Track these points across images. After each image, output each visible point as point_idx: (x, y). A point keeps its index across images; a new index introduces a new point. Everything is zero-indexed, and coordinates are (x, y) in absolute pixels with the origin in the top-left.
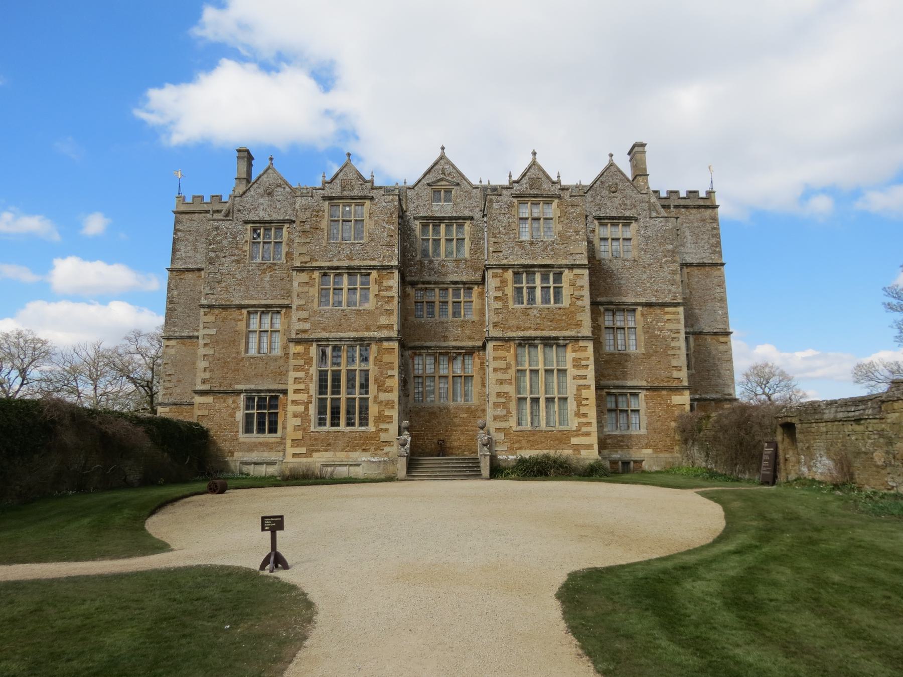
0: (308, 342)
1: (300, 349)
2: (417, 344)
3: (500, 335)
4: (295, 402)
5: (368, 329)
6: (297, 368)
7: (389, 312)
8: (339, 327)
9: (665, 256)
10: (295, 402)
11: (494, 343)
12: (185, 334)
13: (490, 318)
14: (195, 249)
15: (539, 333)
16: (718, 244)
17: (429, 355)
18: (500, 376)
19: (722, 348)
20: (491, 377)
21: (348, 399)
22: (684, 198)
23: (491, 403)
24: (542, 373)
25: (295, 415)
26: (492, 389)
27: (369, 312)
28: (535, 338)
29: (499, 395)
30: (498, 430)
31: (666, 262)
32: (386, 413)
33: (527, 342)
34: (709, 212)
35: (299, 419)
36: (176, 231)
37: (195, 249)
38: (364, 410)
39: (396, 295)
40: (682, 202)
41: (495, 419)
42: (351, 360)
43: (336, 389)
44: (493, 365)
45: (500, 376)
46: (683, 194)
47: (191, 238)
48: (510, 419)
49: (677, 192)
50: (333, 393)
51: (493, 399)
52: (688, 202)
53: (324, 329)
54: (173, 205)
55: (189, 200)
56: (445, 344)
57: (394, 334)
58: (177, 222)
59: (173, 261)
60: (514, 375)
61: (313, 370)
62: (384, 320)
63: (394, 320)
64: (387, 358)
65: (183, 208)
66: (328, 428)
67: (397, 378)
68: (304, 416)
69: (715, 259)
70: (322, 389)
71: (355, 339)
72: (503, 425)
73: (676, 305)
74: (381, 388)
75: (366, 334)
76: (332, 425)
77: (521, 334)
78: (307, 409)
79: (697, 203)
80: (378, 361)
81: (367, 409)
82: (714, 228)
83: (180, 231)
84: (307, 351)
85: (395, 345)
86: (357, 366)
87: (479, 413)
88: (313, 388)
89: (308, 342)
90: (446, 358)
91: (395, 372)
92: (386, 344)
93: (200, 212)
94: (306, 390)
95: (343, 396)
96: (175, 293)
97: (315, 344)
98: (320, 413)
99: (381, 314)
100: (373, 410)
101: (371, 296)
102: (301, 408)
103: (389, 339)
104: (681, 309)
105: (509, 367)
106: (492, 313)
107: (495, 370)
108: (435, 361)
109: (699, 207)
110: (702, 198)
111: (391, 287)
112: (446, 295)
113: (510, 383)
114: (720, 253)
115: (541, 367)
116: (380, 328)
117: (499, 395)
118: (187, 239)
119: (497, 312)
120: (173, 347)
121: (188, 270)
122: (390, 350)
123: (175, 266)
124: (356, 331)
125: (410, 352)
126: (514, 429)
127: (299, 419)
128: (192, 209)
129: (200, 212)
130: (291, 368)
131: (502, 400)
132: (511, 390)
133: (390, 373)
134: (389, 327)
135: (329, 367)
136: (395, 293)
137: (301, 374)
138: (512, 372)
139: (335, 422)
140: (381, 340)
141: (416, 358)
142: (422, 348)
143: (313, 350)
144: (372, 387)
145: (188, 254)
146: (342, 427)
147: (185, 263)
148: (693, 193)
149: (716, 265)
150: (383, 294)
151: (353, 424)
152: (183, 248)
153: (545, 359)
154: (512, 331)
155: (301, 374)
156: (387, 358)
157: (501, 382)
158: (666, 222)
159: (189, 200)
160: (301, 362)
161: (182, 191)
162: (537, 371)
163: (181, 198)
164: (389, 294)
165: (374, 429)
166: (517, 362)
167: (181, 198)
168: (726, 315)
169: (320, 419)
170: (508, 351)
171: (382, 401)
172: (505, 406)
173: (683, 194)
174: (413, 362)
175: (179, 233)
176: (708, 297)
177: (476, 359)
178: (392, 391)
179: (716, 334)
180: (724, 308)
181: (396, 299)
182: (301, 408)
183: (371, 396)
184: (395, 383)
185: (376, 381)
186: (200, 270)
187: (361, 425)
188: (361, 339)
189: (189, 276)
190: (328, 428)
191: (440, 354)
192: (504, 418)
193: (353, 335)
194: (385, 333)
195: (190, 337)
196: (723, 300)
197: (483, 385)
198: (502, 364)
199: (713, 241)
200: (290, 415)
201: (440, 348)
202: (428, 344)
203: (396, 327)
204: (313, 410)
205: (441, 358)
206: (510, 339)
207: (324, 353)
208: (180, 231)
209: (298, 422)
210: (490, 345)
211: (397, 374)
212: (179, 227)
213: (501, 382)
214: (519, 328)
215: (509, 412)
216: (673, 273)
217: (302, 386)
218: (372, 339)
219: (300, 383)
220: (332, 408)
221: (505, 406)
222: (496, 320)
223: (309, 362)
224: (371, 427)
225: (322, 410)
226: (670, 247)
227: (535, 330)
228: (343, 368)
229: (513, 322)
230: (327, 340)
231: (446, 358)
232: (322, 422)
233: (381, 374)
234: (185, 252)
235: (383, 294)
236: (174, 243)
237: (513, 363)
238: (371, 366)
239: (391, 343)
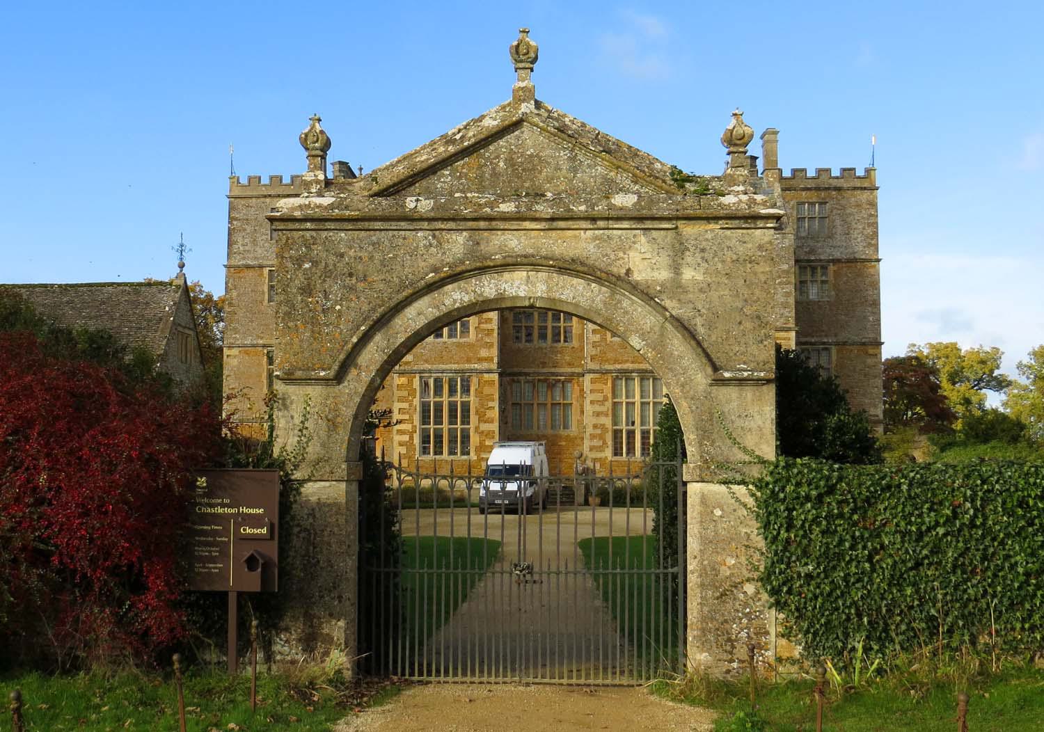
0: (413, 372)
1: (403, 380)
2: (516, 370)
3: (598, 368)
4: (400, 432)
5: (469, 361)
6: (401, 400)
7: (490, 345)
8: (441, 360)
9: (780, 277)
10: (400, 432)
11: (592, 376)
12: (248, 342)
13: (588, 350)
14: (254, 242)
15: (636, 366)
16: (876, 234)
17: (528, 382)
18: (598, 408)
19: (870, 361)
20: (588, 408)
21: (449, 429)
22: (837, 178)
23: (588, 434)
24: (638, 406)
25: (401, 444)
26: (589, 420)
27: (471, 346)
28: (632, 371)
29: (595, 426)
30: (594, 460)
31: (780, 283)
32: (487, 443)
33: (626, 375)
34: (866, 194)
35: (405, 448)
36: (231, 219)
37: (254, 242)
38: (466, 438)
39: (496, 327)
40: (835, 183)
41: (591, 450)
42: (452, 391)
43: (438, 420)
44: (589, 397)
45: (598, 408)
46: (836, 173)
47: (249, 229)
48: (606, 449)
49: (828, 170)
50: (435, 423)
51: (590, 430)
52: (841, 183)
53: (426, 361)
54: (225, 188)
55: (244, 181)
56: (545, 370)
57: (494, 366)
58: (232, 208)
59: (230, 255)
60: (610, 408)
61: (416, 402)
62: (484, 353)
63: (494, 352)
64: (487, 390)
65: (237, 192)
66: (431, 456)
67: (497, 409)
68: (408, 445)
69: (869, 252)
70: (425, 419)
71: (456, 372)
72: (599, 455)
73: (789, 330)
74: (482, 418)
75: (467, 366)
76: (435, 453)
77: (618, 366)
78: (411, 438)
79: (851, 184)
80: (479, 393)
81: (469, 437)
82: (871, 215)
83: (236, 219)
84: (410, 382)
85: (496, 377)
86: (458, 398)
87: (579, 441)
88: (417, 418)
89: (413, 372)
90: (545, 384)
91: (496, 404)
92: (486, 376)
93: (258, 197)
94: (411, 421)
95: (445, 426)
96: (234, 294)
97: (417, 375)
98: (424, 442)
99: (481, 346)
100: (474, 440)
101: (472, 329)
102: (406, 438)
103: (489, 371)
104: (793, 334)
105: (606, 399)
106: (590, 346)
107: (592, 402)
108: (534, 386)
109: (855, 189)
110: (859, 177)
111: (491, 319)
112: (545, 321)
113: (607, 415)
114: (876, 247)
115: (637, 398)
116: (480, 360)
117: (595, 426)
118: (245, 230)
119: (595, 345)
120: (235, 357)
121: (248, 267)
122: (491, 383)
123: (234, 262)
124: (458, 363)
125: (508, 379)
126: (610, 458)
127: (405, 448)
128: (249, 193)
129: (258, 197)
130: (396, 398)
131: (599, 431)
132: (607, 421)
133: (491, 404)
134: (489, 360)
135: (432, 399)
136: (494, 325)
137: (405, 405)
138: (609, 404)
139: (438, 451)
140: (482, 372)
141: (514, 385)
142: (520, 374)
143: (416, 383)
144: (474, 418)
145: (247, 248)
146: (445, 456)
147: (244, 258)
148: (848, 172)
149: (870, 261)
150: (484, 326)
151: (456, 454)
152: (240, 240)
153: (642, 391)
154: (609, 364)
155: (405, 405)
156: (487, 390)
157: (598, 414)
158: (783, 238)
159: (244, 181)
160: (405, 393)
161: (235, 170)
162: (634, 403)
163: (235, 180)
164: (488, 326)
165: (475, 458)
166: (614, 395)
167: (235, 180)
168: (877, 322)
169: (424, 448)
170: (606, 384)
171: (483, 432)
172: (601, 437)
173: (836, 173)
174: (511, 389)
175: (235, 223)
176: (857, 301)
177: (576, 385)
178: (492, 421)
179: (864, 344)
180: (877, 314)
181: (496, 332)
182: (406, 438)
183: (472, 426)
184: (495, 413)
185: (477, 412)
186: (261, 267)
187: (463, 453)
188: (463, 371)
189: (250, 273)
190: (431, 456)
191: (539, 380)
192: (601, 449)
193: (454, 367)
194: (485, 366)
195: (254, 346)
196: (876, 304)
197: (582, 412)
198: (599, 397)
199: (869, 231)
200: (395, 444)
201: (539, 374)
202: (526, 370)
203: (496, 360)
204: (417, 440)
205: (540, 384)
206: (608, 372)
207: (427, 384)
208: (236, 219)
209: (403, 450)
210: (588, 377)
211: (497, 405)
212: (234, 215)
213: (598, 414)
214: (616, 361)
215: (605, 443)
216: (787, 294)
217: (407, 417)
218: (471, 371)
219: (404, 413)
220: (435, 436)
221: (601, 437)
222: (594, 353)
223: (412, 393)
224: (473, 456)
225: (425, 439)
226: (785, 267)
227: (633, 362)
228: (445, 399)
229: (610, 355)
230: (430, 371)
231: (545, 384)
232: (425, 451)
233: (482, 405)
234: (243, 245)
235: (484, 326)
236: (229, 234)
237: (610, 395)
238: (472, 399)
239: (491, 375)
